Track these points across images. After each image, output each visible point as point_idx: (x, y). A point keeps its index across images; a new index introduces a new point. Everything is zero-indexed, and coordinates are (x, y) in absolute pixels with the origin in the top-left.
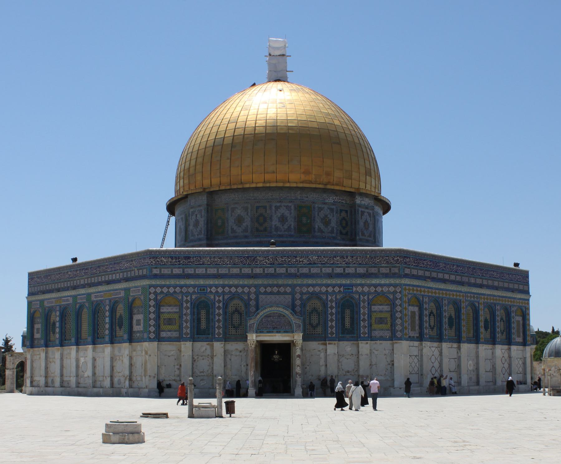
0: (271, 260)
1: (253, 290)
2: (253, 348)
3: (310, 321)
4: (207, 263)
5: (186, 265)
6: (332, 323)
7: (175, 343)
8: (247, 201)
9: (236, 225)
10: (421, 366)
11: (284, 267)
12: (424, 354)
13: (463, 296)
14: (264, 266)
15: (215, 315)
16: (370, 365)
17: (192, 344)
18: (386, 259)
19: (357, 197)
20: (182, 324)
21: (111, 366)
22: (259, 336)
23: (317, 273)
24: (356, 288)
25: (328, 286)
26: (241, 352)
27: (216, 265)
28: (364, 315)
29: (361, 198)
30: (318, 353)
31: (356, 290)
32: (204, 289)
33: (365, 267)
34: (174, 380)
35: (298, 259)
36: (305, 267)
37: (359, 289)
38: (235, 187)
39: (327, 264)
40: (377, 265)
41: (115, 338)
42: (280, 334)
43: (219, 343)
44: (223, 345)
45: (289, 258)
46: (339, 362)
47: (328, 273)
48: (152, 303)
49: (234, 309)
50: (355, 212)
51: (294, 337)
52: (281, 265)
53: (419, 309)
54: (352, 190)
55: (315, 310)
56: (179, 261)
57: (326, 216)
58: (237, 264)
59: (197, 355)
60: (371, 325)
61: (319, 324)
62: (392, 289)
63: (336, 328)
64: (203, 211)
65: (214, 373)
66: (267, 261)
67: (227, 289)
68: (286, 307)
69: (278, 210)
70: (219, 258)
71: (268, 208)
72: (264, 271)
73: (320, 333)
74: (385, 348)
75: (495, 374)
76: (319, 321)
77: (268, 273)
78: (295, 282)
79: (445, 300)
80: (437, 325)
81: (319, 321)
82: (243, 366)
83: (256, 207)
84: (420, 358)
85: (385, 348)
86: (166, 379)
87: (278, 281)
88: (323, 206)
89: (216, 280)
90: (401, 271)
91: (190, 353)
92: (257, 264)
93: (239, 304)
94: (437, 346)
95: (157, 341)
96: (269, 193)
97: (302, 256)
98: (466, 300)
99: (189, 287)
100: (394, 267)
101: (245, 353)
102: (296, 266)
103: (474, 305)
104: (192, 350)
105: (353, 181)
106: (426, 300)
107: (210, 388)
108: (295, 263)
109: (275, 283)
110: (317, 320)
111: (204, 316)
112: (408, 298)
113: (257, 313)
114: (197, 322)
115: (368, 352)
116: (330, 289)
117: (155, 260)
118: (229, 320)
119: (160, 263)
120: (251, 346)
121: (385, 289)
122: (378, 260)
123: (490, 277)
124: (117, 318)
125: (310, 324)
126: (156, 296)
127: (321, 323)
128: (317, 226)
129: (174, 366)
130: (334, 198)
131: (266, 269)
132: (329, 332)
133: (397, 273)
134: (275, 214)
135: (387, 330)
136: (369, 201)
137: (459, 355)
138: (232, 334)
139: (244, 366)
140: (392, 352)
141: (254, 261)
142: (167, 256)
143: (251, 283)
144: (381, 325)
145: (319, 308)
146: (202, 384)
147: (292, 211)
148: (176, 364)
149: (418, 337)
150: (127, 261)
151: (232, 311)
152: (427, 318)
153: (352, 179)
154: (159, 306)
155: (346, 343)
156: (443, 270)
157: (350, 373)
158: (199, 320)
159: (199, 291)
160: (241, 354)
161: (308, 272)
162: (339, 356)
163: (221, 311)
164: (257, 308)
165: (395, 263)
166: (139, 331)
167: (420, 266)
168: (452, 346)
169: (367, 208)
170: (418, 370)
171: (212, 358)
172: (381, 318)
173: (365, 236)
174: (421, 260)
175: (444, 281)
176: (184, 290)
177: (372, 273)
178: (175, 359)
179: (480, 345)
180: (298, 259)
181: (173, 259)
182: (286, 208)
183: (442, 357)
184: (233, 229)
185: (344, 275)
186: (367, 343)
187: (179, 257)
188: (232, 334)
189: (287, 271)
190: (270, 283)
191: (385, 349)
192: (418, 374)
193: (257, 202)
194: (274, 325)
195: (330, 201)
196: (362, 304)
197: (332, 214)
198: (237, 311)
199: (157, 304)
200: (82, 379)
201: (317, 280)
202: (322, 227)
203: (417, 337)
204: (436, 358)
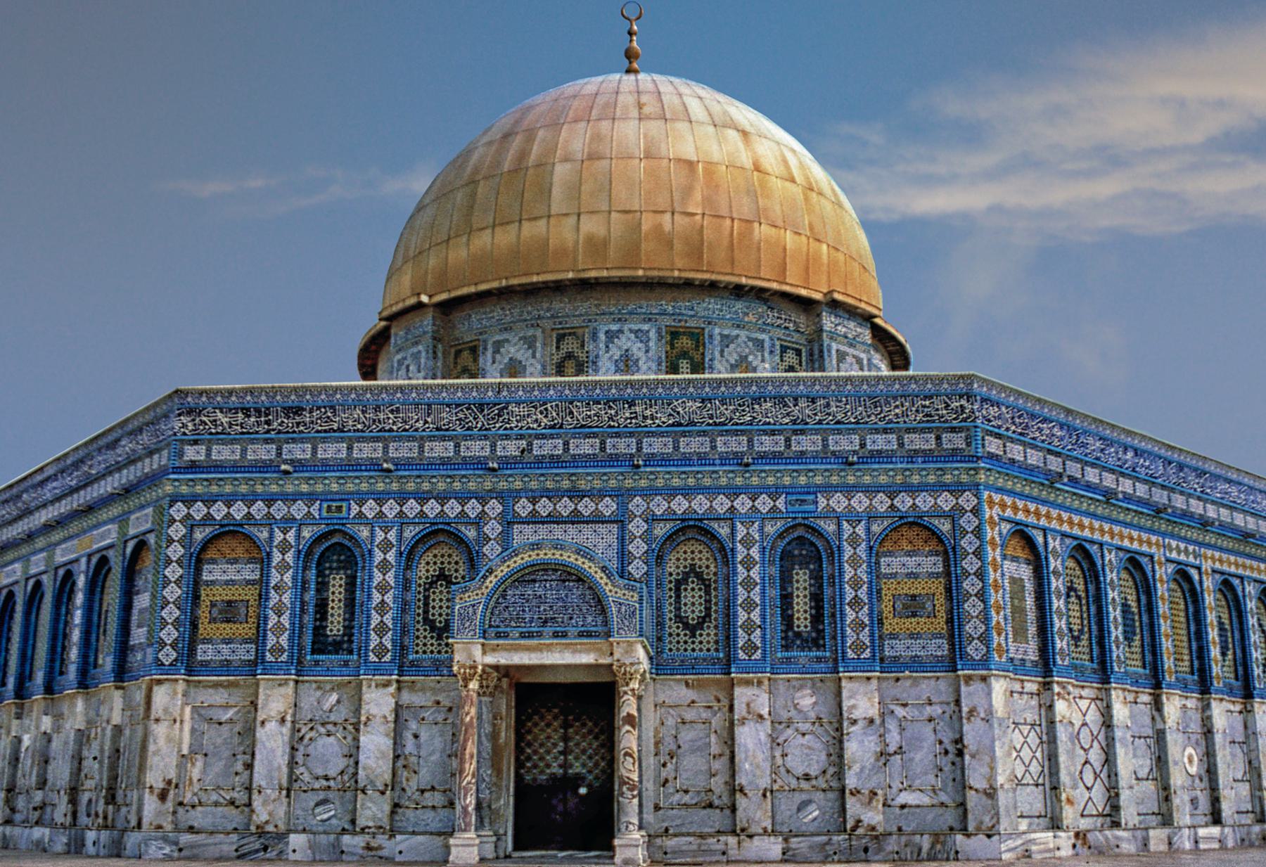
0: (554, 414)
1: (494, 508)
5: (288, 432)
13: (1157, 544)
14: (530, 431)
16: (882, 754)
18: (924, 406)
20: (266, 618)
22: (495, 649)
25: (735, 494)
27: (380, 431)
28: (856, 585)
32: (341, 507)
35: (638, 409)
36: (661, 435)
37: (839, 502)
41: (93, 671)
45: (610, 407)
49: (433, 571)
50: (821, 351)
52: (584, 431)
55: (693, 572)
56: (268, 423)
58: (447, 430)
59: (311, 720)
60: (881, 622)
62: (946, 501)
64: (423, 354)
67: (412, 508)
70: (392, 411)
76: (708, 609)
81: (708, 609)
84: (1044, 731)
88: (735, 332)
92: (508, 426)
99: (295, 501)
103: (1188, 579)
106: (1054, 543)
110: (700, 604)
112: (1000, 534)
113: (487, 571)
114: (316, 612)
115: (874, 712)
117: (193, 420)
118: (419, 607)
122: (897, 411)
123: (1222, 498)
125: (679, 618)
126: (191, 528)
127: (714, 616)
134: (607, 352)
135: (935, 636)
136: (859, 330)
137: (1160, 726)
140: (957, 709)
141: (501, 419)
144: (913, 620)
145: (708, 567)
146: (318, 818)
151: (427, 578)
152: (1062, 601)
156: (1098, 459)
157: (814, 782)
158: (322, 608)
159: (325, 514)
165: (954, 419)
172: (914, 597)
176: (279, 510)
180: (638, 409)
181: (249, 416)
182: (637, 337)
183: (1113, 730)
185: (786, 458)
187: (268, 409)
192: (1043, 785)
194: (545, 610)
196: (848, 552)
197: (759, 354)
203: (1035, 664)
204: (1095, 733)
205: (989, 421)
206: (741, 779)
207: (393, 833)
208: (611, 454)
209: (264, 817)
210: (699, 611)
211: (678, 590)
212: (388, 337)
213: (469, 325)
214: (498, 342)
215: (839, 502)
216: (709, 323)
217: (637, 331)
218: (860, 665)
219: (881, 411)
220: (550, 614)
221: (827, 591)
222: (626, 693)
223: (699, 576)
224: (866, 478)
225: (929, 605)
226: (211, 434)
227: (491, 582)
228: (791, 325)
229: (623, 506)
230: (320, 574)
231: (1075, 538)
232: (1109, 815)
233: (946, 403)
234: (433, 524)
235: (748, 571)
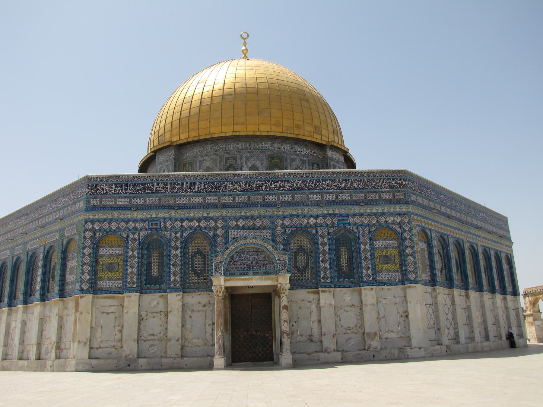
1: (220, 223)
2: (220, 298)
4: (162, 191)
5: (134, 193)
6: (325, 264)
7: (116, 295)
8: (215, 152)
10: (437, 318)
11: (260, 194)
12: (439, 303)
14: (235, 193)
15: (170, 256)
17: (140, 296)
18: (388, 182)
19: (328, 150)
20: (127, 270)
21: (39, 330)
22: (229, 280)
23: (302, 201)
24: (353, 219)
26: (205, 306)
28: (366, 253)
30: (308, 304)
32: (157, 223)
33: (362, 193)
34: (114, 347)
35: (278, 184)
37: (357, 220)
38: (203, 137)
39: (315, 190)
40: (378, 190)
42: (257, 277)
43: (175, 294)
44: (180, 297)
45: (266, 183)
46: (336, 316)
47: (317, 201)
48: (88, 243)
49: (195, 249)
51: (277, 281)
52: (256, 192)
53: (428, 246)
54: (324, 143)
55: (301, 248)
56: (125, 189)
58: (200, 192)
59: (146, 312)
61: (308, 267)
62: (398, 219)
63: (331, 271)
64: (171, 165)
65: (168, 336)
66: (238, 187)
67: (186, 224)
68: (264, 239)
71: (238, 159)
72: (234, 200)
73: (310, 278)
74: (394, 295)
75: (499, 327)
76: (308, 263)
77: (239, 202)
78: (275, 213)
80: (445, 268)
81: (308, 263)
82: (207, 325)
83: (226, 158)
84: (434, 307)
85: (394, 295)
86: (101, 346)
87: (253, 211)
88: (295, 157)
89: (172, 211)
91: (136, 309)
93: (202, 243)
94: (448, 293)
95: (92, 292)
97: (282, 180)
100: (398, 192)
101: (211, 308)
102: (275, 192)
104: (140, 305)
106: (434, 235)
107: (162, 357)
109: (250, 214)
111: (157, 259)
115: (374, 301)
116: (320, 221)
117: (94, 188)
119: (101, 192)
120: (218, 295)
121: (390, 219)
122: (378, 184)
123: (482, 219)
124: (51, 269)
125: (296, 267)
127: (310, 266)
129: (114, 327)
131: (237, 198)
133: (403, 199)
134: (246, 164)
135: (396, 271)
136: (340, 157)
137: (468, 304)
138: (193, 283)
139: (209, 325)
140: (405, 299)
142: (110, 183)
145: (307, 246)
146: (151, 352)
147: (264, 161)
148: (117, 324)
150: (65, 195)
154: (97, 246)
155: (344, 290)
156: (445, 203)
157: (352, 330)
160: (205, 309)
162: (336, 308)
163: (178, 252)
164: (226, 242)
165: (399, 187)
166: (71, 281)
167: (424, 194)
170: (434, 323)
171: (166, 315)
172: (387, 256)
175: (449, 217)
176: (131, 225)
177: (371, 200)
178: (116, 318)
179: (484, 293)
180: (278, 184)
181: (118, 187)
182: (257, 159)
186: (372, 289)
188: (193, 283)
189: (264, 199)
190: (243, 214)
192: (435, 328)
193: (227, 153)
194: (249, 264)
195: (302, 153)
198: (199, 252)
199: (94, 244)
200: (10, 349)
201: (303, 210)
206: (324, 330)
207: (182, 356)
208: (267, 202)
209: (128, 352)
211: (295, 256)
212: (155, 158)
213: (190, 154)
215: (357, 220)
216: (285, 153)
218: (368, 284)
219: (372, 185)
221: (355, 255)
222: (284, 297)
223: (304, 250)
226: (102, 194)
227: (227, 253)
229: (273, 222)
230: (148, 251)
231: (440, 233)
232: (455, 339)
233: (395, 181)
234: (195, 230)
235: (324, 247)
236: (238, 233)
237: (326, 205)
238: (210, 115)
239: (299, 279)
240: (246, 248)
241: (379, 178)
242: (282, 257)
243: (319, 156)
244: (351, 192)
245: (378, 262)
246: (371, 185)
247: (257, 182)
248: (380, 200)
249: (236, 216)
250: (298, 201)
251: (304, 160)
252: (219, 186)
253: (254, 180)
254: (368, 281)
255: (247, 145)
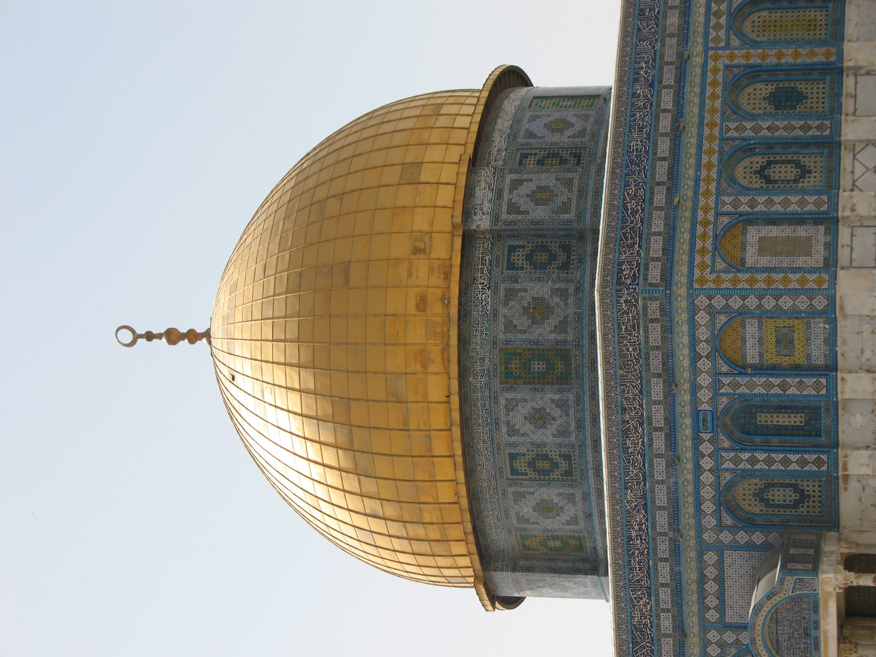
0: (639, 593)
1: (713, 636)
3: (788, 506)
9: (558, 515)
11: (655, 565)
14: (653, 609)
18: (626, 329)
19: (474, 227)
23: (668, 492)
28: (772, 386)
29: (475, 214)
31: (707, 403)
33: (648, 381)
35: (634, 534)
36: (654, 518)
37: (704, 395)
39: (645, 468)
40: (643, 351)
42: (822, 622)
45: (633, 553)
52: (650, 573)
57: (525, 310)
62: (702, 318)
66: (641, 602)
69: (519, 430)
71: (512, 451)
72: (668, 611)
74: (856, 333)
76: (789, 485)
77: (672, 602)
78: (692, 542)
79: (728, 129)
81: (789, 485)
83: (512, 474)
85: (856, 333)
88: (502, 320)
90: (656, 295)
92: (649, 625)
94: (851, 155)
96: (479, 447)
97: (627, 525)
98: (727, 46)
100: (647, 311)
102: (651, 540)
105: (435, 228)
108: (645, 540)
109: (694, 587)
121: (703, 333)
128: (553, 336)
130: (480, 287)
132: (815, 469)
133: (660, 304)
135: (809, 328)
136: (483, 184)
143: (696, 640)
144: (796, 343)
145: (756, 484)
149: (826, 230)
153: (429, 230)
161: (665, 514)
165: (636, 308)
168: (852, 96)
169: (499, 194)
172: (778, 341)
173: (569, 199)
174: (624, 220)
177: (663, 366)
182: (513, 410)
184: (567, 521)
185: (670, 432)
186: (843, 379)
189: (666, 560)
190: (695, 597)
191: (859, 333)
194: (798, 634)
195: (489, 300)
196: (743, 390)
202: (553, 321)
203: (827, 232)
205: (634, 275)
210: (789, 492)
214: (518, 521)
215: (704, 395)
216: (495, 343)
217: (507, 409)
220: (801, 631)
223: (762, 491)
224: (685, 376)
225: (784, 331)
228: (487, 258)
229: (710, 547)
233: (623, 313)
236: (731, 607)
237: (675, 452)
238: (408, 502)
239: (819, 502)
240: (770, 638)
241: (616, 346)
242: (787, 586)
243: (488, 245)
244: (648, 402)
245: (790, 359)
246: (633, 362)
247: (631, 569)
248: (664, 348)
249: (699, 610)
250: (668, 500)
251: (506, 295)
252: (641, 634)
253: (627, 573)
254: (827, 387)
255: (482, 432)
